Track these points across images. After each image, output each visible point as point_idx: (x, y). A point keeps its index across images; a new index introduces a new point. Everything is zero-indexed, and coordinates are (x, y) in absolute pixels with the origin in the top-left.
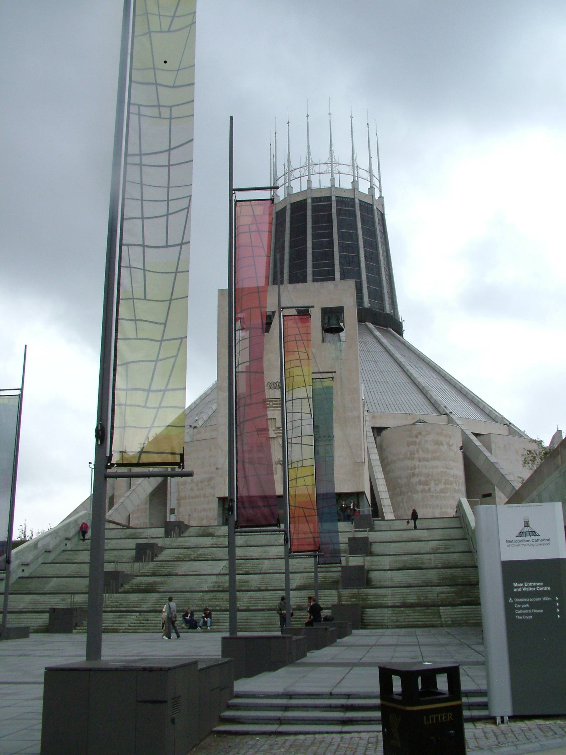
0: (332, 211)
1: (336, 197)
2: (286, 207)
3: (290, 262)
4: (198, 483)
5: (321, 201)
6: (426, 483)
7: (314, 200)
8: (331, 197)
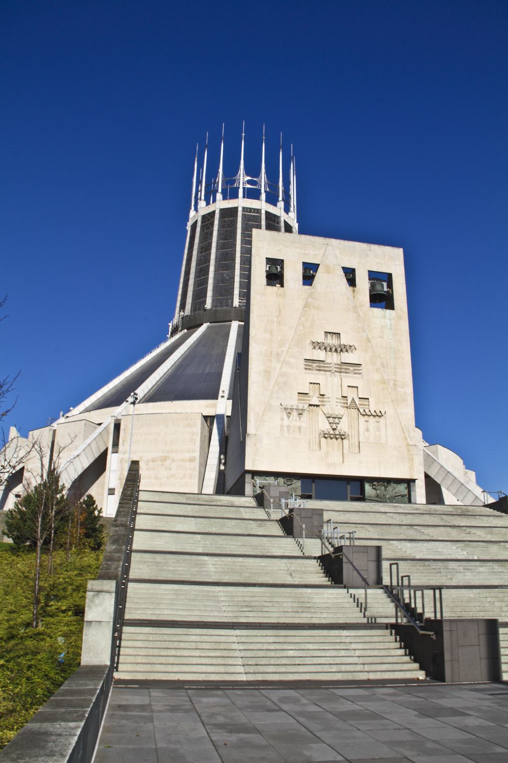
0: (261, 222)
2: (214, 212)
3: (216, 262)
4: (148, 461)
5: (250, 212)
7: (244, 209)
8: (261, 210)
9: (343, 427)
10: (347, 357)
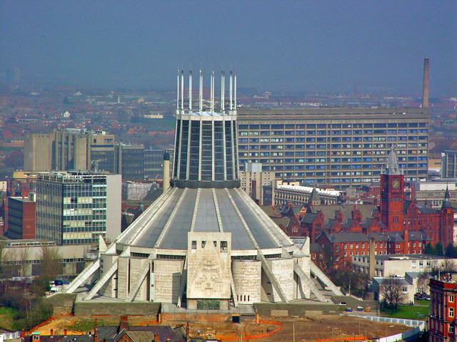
1: (215, 122)
6: (248, 283)
9: (211, 286)
10: (213, 268)
